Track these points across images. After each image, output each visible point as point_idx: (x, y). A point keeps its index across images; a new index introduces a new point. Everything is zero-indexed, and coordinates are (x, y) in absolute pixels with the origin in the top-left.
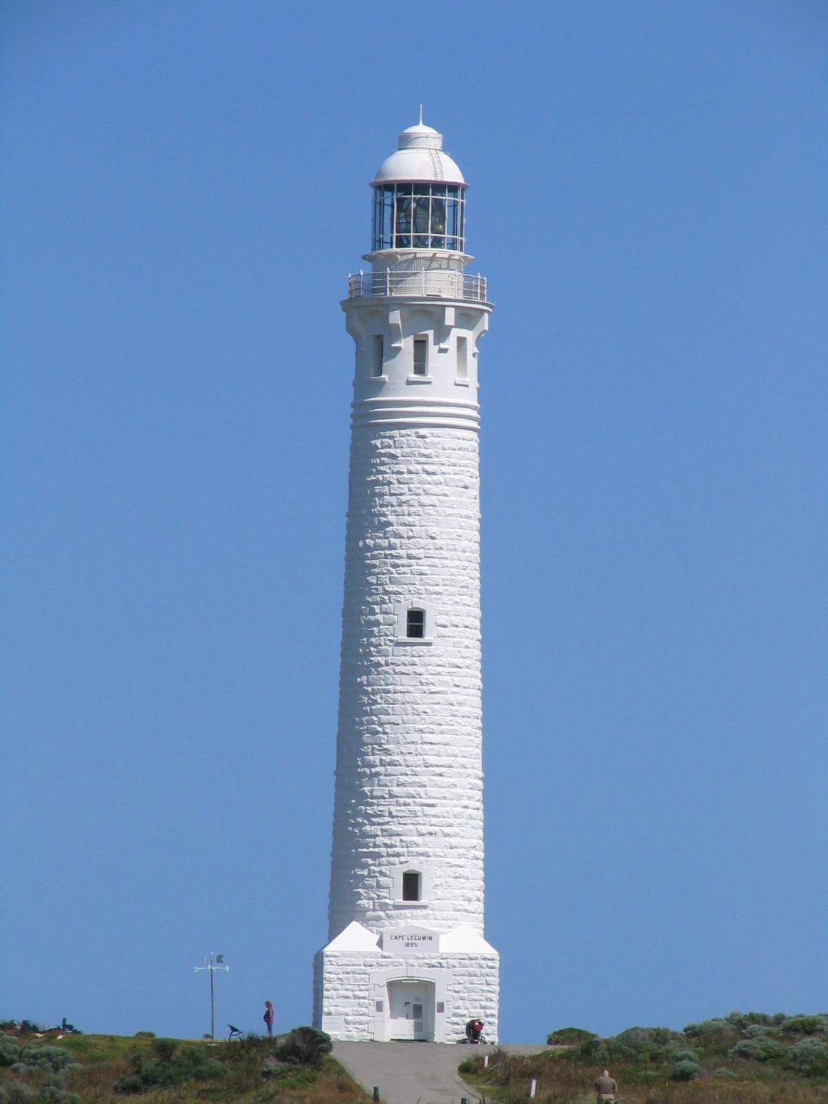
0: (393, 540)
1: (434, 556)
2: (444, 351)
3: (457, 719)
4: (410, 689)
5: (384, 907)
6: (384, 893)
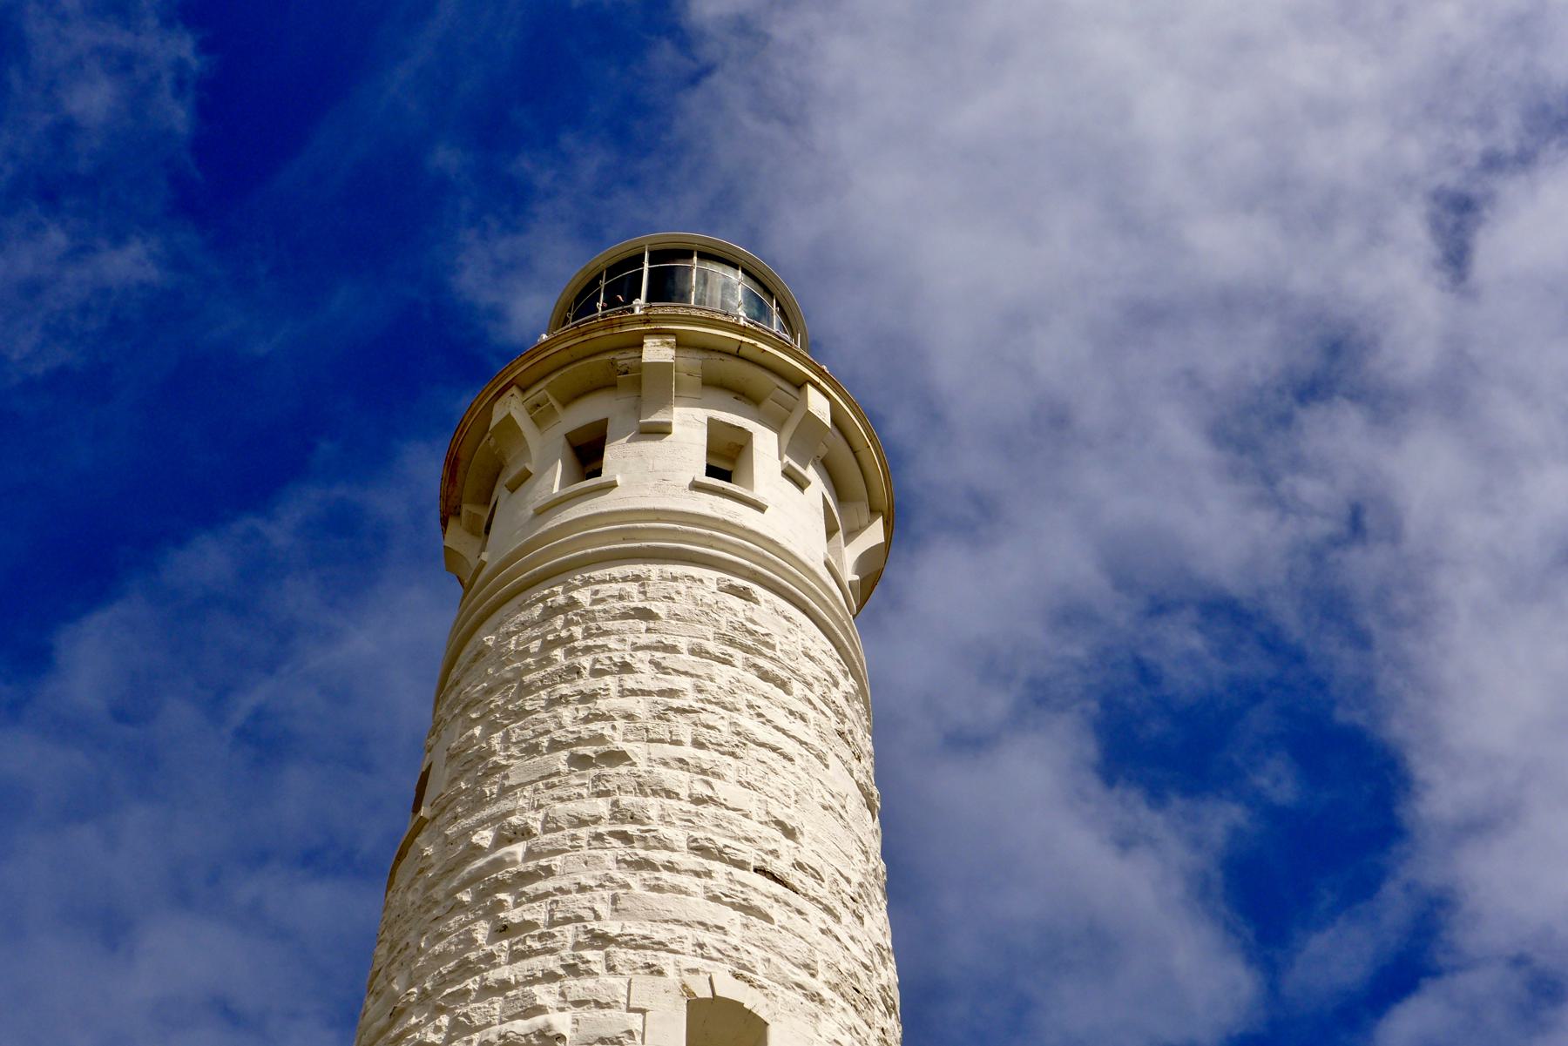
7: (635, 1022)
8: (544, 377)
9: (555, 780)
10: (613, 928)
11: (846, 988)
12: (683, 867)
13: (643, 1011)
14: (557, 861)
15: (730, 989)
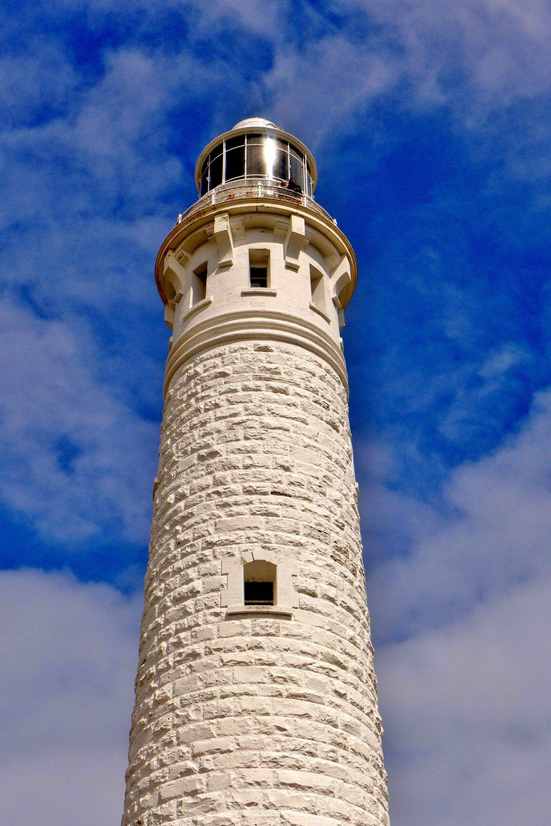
1: (290, 493)
2: (294, 268)
3: (341, 752)
4: (251, 688)
7: (224, 579)
8: (185, 238)
9: (193, 468)
10: (214, 538)
11: (314, 533)
12: (241, 502)
13: (227, 574)
14: (195, 509)
15: (260, 555)
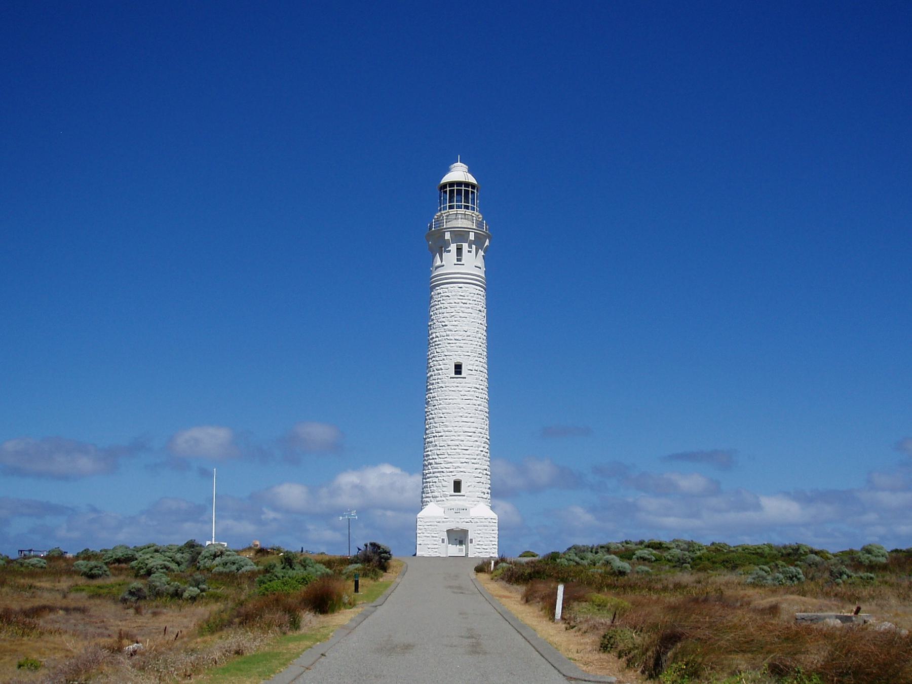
0: (448, 333)
2: (470, 252)
5: (445, 496)
6: (444, 489)
